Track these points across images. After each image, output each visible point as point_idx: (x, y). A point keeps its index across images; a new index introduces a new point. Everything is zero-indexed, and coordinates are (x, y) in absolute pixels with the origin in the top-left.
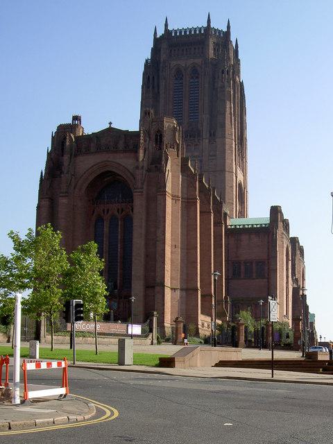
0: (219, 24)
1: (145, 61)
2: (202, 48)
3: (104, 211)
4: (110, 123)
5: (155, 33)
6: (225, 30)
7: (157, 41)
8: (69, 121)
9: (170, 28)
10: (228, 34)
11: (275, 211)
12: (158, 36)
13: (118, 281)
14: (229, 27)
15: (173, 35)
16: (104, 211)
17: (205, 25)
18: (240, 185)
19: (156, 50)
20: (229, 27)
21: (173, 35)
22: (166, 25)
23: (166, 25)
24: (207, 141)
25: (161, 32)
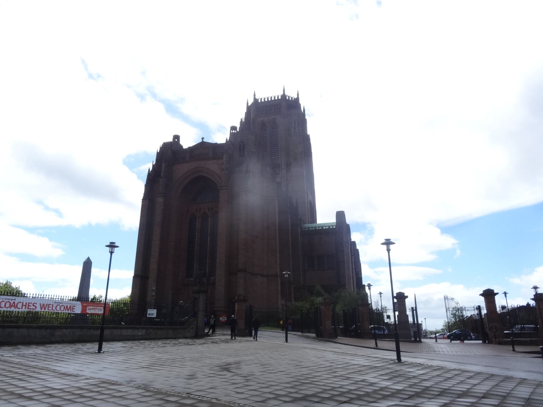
0: (291, 94)
1: (240, 120)
2: (280, 108)
3: (197, 210)
4: (203, 138)
5: (248, 103)
6: (296, 97)
7: (249, 108)
8: (171, 139)
9: (257, 97)
10: (297, 100)
11: (340, 215)
12: (249, 104)
13: (207, 270)
14: (298, 95)
15: (259, 101)
16: (197, 210)
17: (282, 93)
18: (310, 203)
19: (248, 114)
20: (298, 95)
21: (259, 101)
22: (255, 95)
23: (255, 95)
24: (285, 170)
25: (251, 101)
